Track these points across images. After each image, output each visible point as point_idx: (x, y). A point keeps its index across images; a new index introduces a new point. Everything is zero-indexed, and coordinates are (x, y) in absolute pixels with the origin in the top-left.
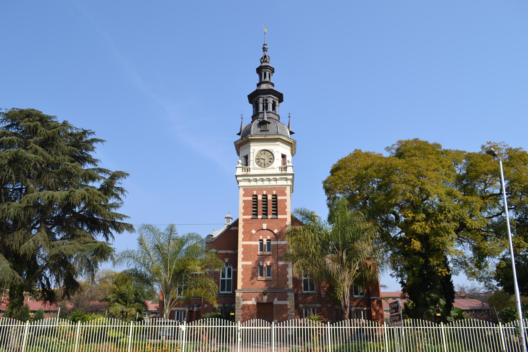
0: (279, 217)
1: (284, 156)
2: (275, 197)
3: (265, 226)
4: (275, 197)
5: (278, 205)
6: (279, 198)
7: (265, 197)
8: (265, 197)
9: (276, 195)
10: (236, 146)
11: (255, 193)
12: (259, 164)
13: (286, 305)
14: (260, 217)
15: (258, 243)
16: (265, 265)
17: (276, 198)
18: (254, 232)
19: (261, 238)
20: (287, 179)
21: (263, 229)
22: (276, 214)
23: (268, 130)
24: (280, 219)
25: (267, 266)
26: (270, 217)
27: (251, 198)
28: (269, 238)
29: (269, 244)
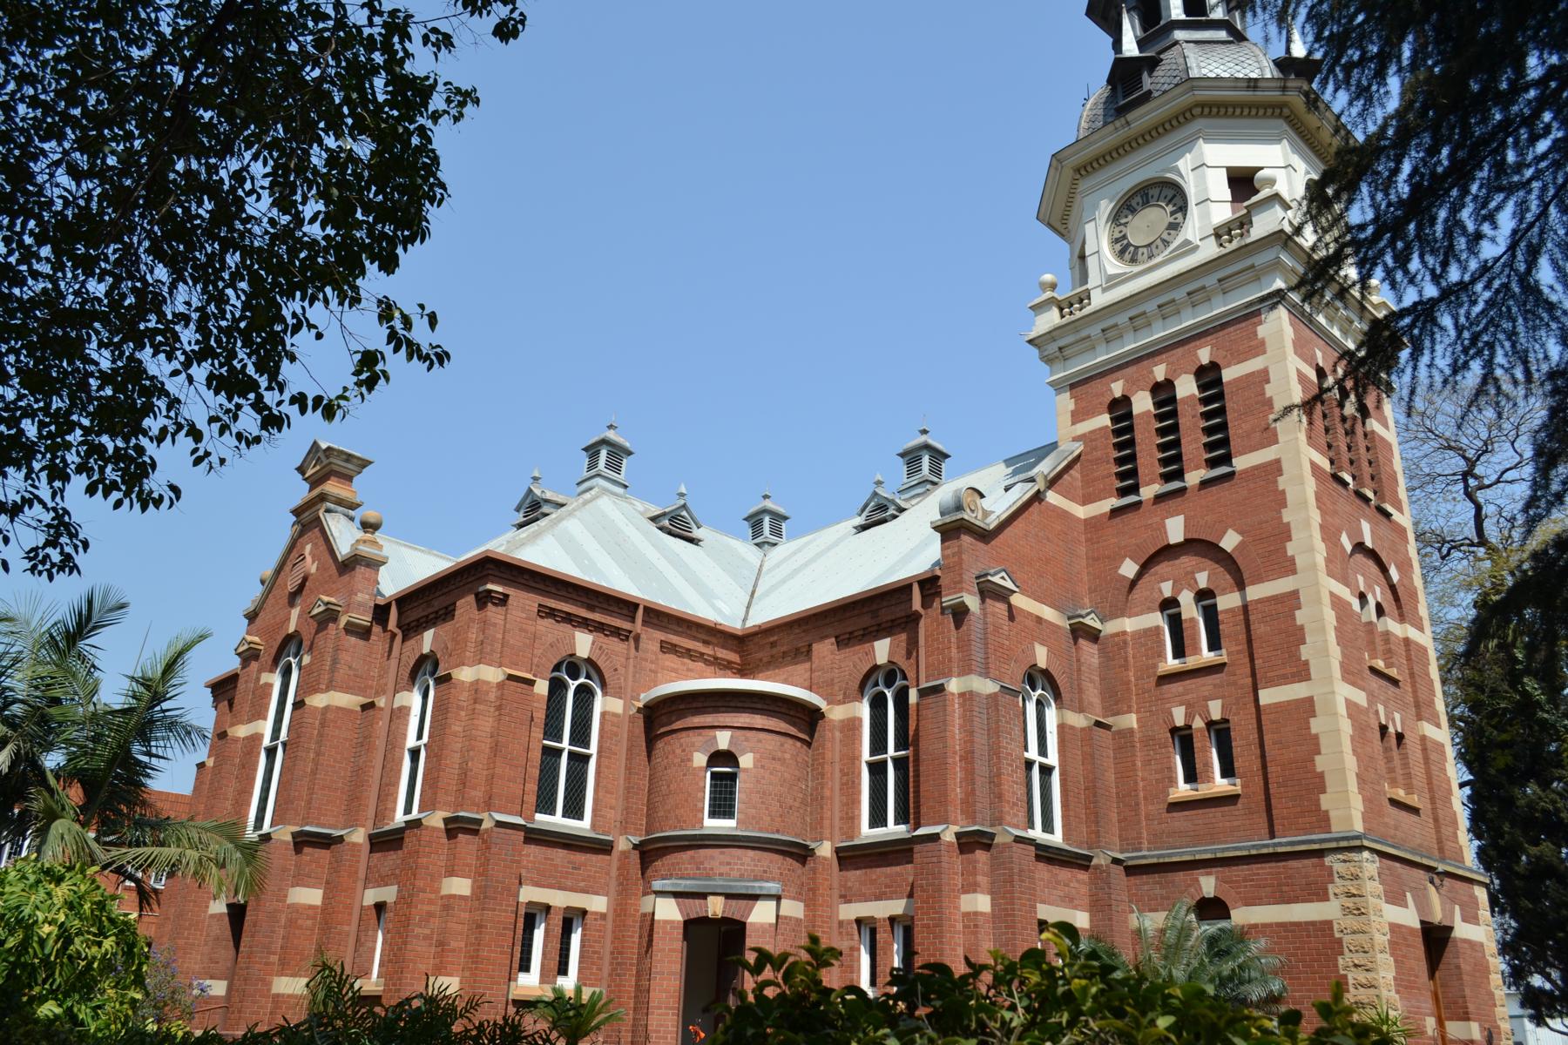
0: (1240, 463)
1: (1242, 182)
2: (1209, 377)
3: (1175, 530)
4: (1209, 377)
5: (1229, 405)
6: (1228, 375)
7: (1163, 392)
8: (1163, 392)
9: (1214, 367)
10: (1050, 225)
11: (1117, 389)
12: (1127, 256)
13: (1329, 924)
14: (1148, 492)
15: (1157, 619)
16: (1198, 723)
17: (1218, 381)
18: (1129, 569)
19: (1167, 590)
20: (1256, 274)
21: (1169, 547)
22: (1226, 459)
23: (1150, 92)
24: (1245, 471)
25: (1210, 724)
26: (1193, 477)
27: (1104, 420)
28: (1202, 580)
29: (1211, 615)
